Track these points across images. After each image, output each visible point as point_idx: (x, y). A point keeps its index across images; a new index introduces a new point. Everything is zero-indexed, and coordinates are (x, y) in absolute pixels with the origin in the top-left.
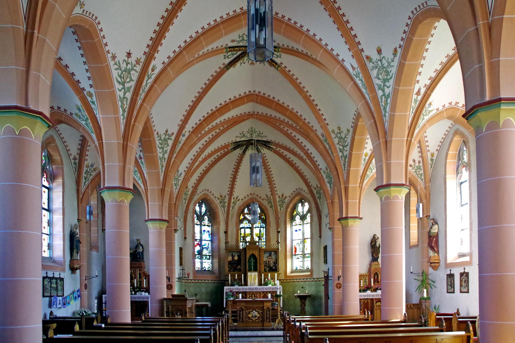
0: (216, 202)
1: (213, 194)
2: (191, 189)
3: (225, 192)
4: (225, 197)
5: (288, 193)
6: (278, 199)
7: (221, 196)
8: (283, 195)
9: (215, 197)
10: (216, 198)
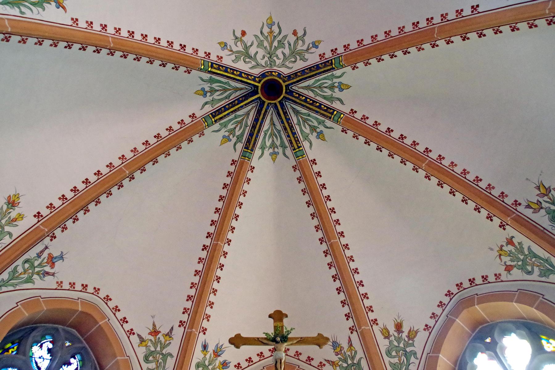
0: (129, 351)
1: (125, 320)
2: (29, 221)
3: (171, 316)
4: (169, 335)
5: (417, 317)
6: (383, 344)
7: (155, 332)
8: (399, 327)
9: (131, 332)
10: (135, 339)
